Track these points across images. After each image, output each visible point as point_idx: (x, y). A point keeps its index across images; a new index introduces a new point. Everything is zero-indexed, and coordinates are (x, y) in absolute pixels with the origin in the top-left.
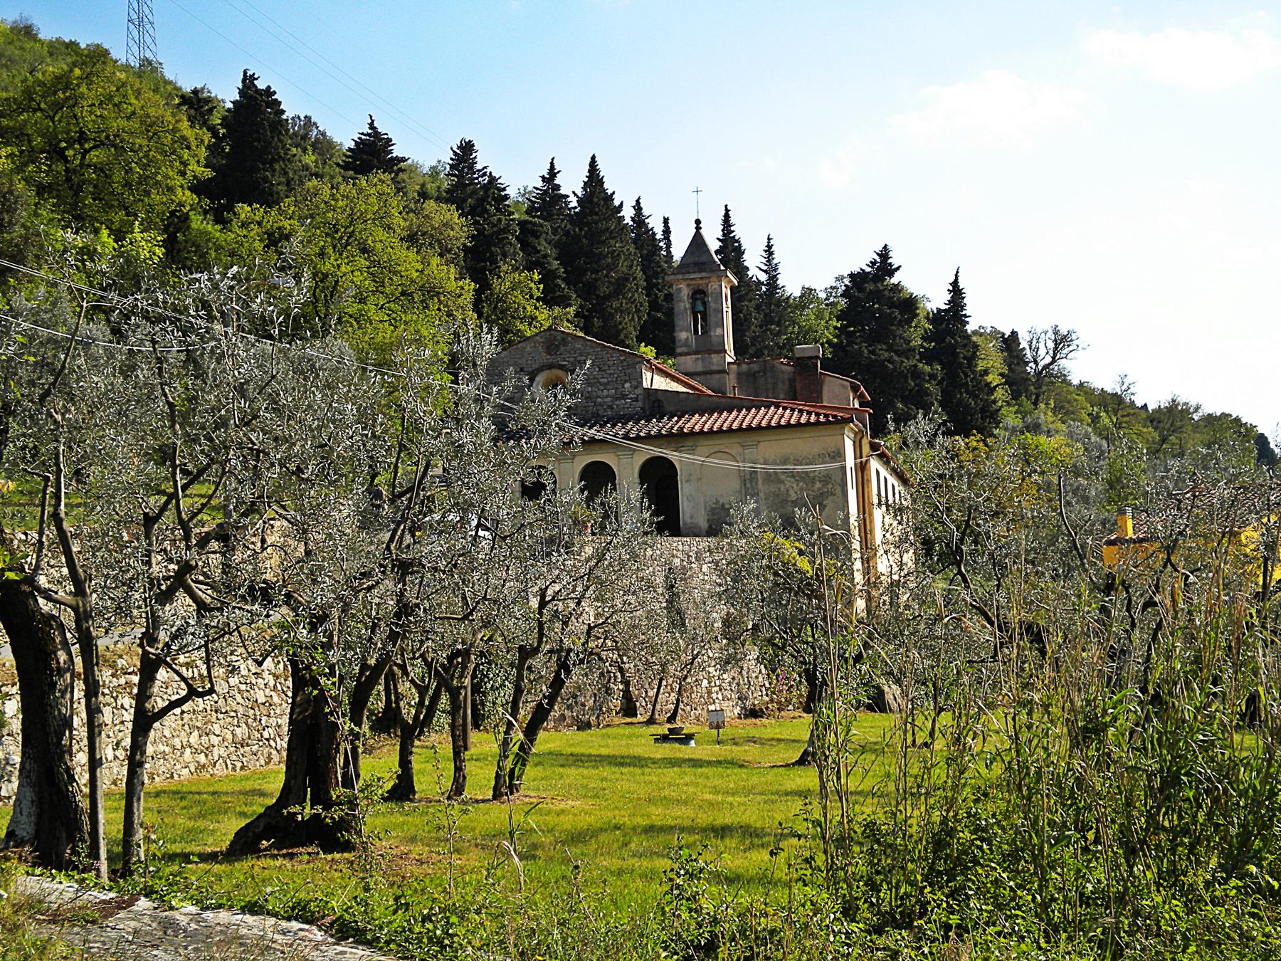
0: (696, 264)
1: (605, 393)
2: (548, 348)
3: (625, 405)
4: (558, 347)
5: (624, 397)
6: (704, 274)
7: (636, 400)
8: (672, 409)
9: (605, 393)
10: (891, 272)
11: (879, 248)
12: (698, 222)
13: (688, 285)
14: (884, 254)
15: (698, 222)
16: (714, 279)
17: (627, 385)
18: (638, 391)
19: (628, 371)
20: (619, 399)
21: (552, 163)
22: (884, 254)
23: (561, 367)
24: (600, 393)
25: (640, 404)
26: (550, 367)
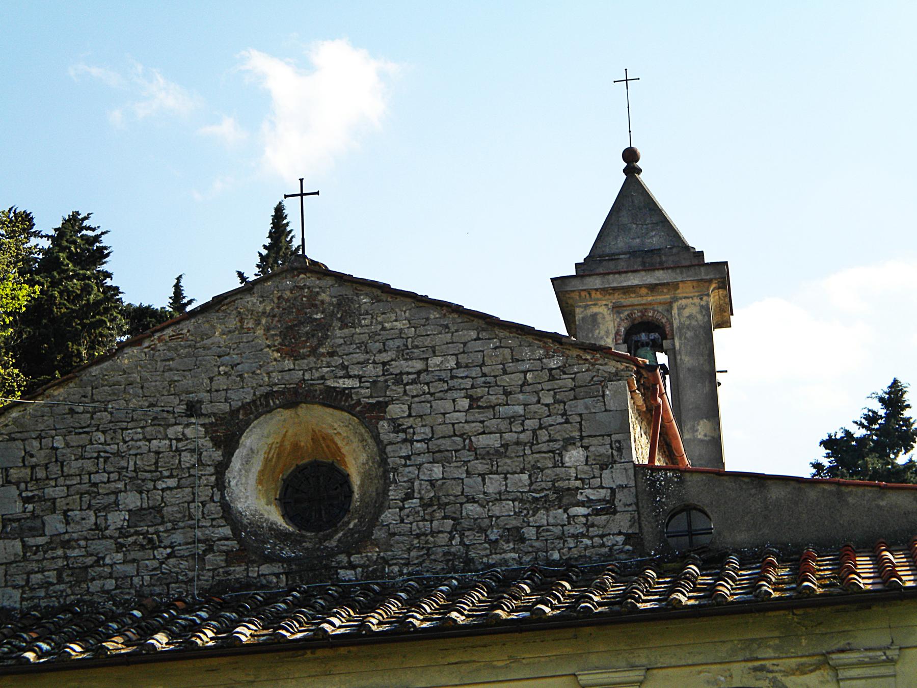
0: (633, 253)
1: (494, 485)
2: (289, 332)
3: (567, 529)
4: (323, 327)
5: (563, 497)
6: (660, 276)
7: (609, 508)
8: (742, 537)
9: (494, 485)
10: (905, 439)
11: (882, 387)
12: (630, 156)
13: (617, 308)
14: (894, 399)
15: (630, 156)
16: (686, 289)
17: (574, 456)
18: (615, 477)
19: (580, 406)
20: (546, 504)
21: (178, 287)
22: (894, 399)
23: (334, 399)
24: (473, 485)
25: (622, 522)
26: (294, 397)
